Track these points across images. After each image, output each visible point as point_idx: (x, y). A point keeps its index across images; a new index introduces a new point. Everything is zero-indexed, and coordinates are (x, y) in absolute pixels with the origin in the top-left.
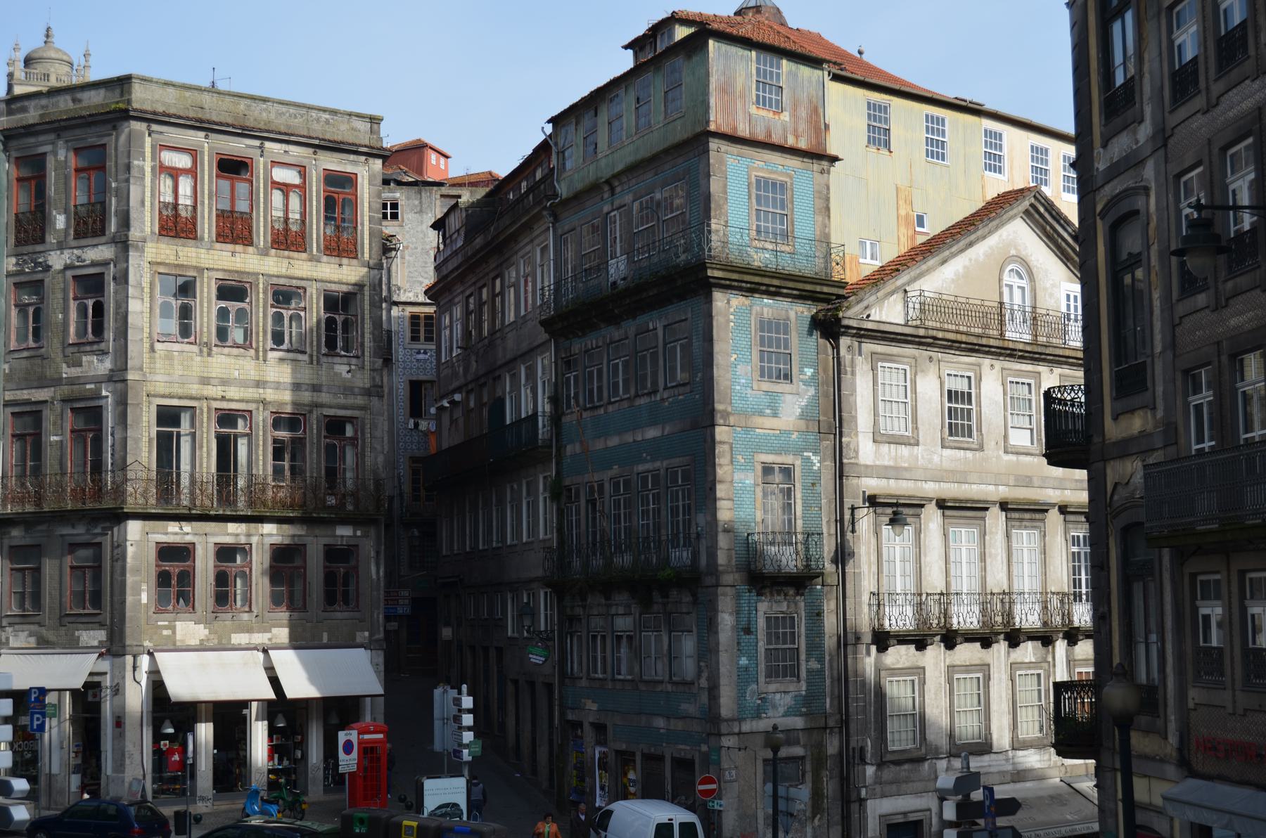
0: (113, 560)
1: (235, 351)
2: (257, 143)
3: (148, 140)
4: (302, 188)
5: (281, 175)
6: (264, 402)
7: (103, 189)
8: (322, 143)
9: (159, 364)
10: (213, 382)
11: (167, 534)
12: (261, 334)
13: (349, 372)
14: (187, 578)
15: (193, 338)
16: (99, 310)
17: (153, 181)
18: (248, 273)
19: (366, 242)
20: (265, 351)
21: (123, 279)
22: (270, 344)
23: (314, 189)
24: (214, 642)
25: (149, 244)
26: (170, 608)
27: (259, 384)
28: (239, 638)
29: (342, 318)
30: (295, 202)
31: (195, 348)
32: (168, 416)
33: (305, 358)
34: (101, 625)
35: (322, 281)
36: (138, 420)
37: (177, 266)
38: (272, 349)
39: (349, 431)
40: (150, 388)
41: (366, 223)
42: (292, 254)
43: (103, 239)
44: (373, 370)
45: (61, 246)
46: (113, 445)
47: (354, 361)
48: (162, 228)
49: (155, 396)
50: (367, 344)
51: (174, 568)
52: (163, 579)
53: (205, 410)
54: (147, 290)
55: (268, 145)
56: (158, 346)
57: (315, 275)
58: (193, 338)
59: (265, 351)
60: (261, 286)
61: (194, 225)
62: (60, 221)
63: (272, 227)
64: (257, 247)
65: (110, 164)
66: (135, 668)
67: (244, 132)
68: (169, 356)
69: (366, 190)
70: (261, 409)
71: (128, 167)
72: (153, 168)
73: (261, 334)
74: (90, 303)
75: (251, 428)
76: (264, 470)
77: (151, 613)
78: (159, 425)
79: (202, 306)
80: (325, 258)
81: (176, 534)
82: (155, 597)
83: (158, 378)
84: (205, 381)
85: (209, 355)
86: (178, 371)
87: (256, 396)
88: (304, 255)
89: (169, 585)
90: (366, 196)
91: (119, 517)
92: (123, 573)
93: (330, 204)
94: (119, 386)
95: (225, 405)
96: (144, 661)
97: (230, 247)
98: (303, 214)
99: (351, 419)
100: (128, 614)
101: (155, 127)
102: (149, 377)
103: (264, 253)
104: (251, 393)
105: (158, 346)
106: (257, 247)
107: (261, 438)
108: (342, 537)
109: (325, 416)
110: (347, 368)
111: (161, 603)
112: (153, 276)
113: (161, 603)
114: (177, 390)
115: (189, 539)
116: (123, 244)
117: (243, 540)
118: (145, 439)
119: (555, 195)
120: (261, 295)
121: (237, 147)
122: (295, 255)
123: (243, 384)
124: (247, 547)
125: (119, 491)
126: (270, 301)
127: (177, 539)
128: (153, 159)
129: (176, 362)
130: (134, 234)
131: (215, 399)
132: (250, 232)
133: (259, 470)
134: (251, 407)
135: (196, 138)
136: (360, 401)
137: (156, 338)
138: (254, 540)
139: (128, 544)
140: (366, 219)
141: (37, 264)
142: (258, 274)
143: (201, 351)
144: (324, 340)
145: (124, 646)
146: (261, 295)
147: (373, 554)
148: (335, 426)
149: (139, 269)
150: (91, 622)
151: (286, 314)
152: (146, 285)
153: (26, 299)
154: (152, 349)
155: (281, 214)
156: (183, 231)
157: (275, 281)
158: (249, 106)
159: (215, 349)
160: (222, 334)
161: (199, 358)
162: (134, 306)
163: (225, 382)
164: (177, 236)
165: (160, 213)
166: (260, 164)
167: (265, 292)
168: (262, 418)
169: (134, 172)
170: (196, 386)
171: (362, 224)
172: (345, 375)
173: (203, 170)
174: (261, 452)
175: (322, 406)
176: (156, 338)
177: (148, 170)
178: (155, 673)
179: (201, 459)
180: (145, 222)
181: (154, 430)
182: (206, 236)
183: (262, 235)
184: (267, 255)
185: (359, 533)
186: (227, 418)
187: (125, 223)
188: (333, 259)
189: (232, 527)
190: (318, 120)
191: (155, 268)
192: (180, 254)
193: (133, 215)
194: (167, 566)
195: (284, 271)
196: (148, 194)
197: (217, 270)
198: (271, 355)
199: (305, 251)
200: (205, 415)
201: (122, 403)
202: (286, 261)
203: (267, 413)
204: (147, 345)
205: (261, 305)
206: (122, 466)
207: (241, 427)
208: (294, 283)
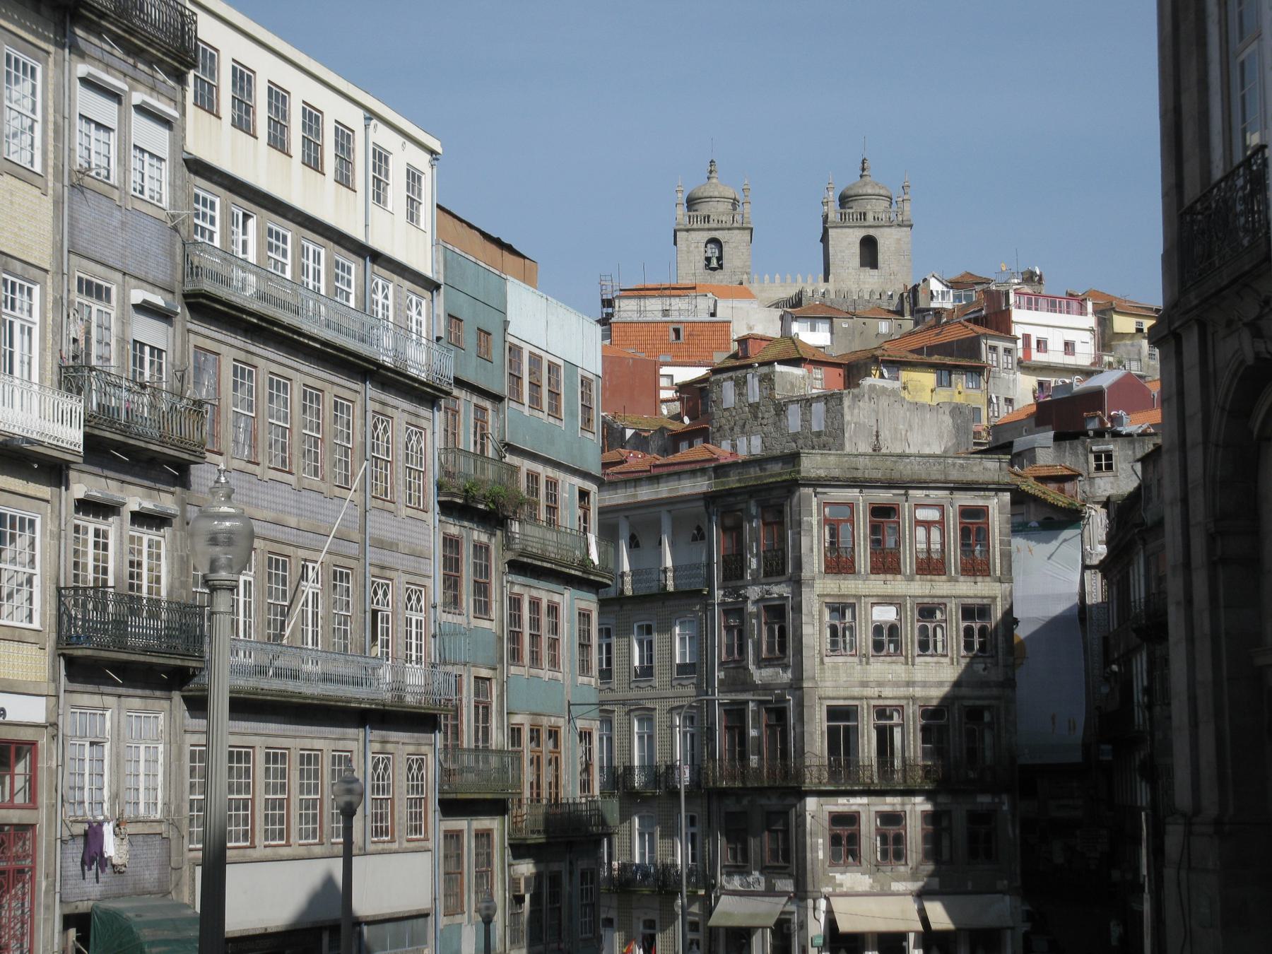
0: (797, 826)
1: (888, 659)
2: (903, 492)
3: (814, 500)
4: (941, 524)
5: (922, 514)
6: (913, 698)
7: (783, 539)
8: (956, 485)
9: (828, 674)
10: (871, 684)
11: (837, 805)
12: (909, 644)
13: (985, 669)
14: (854, 839)
15: (854, 651)
16: (783, 632)
17: (819, 532)
18: (898, 596)
19: (998, 561)
20: (913, 657)
21: (798, 609)
22: (917, 651)
23: (952, 522)
24: (877, 889)
25: (817, 581)
26: (842, 862)
27: (909, 684)
28: (897, 886)
29: (978, 625)
30: (935, 534)
31: (856, 659)
32: (835, 713)
33: (947, 660)
34: (790, 876)
35: (960, 597)
36: (812, 718)
37: (839, 596)
38: (919, 655)
39: (987, 717)
40: (822, 692)
41: (997, 546)
42: (933, 577)
43: (783, 578)
44: (1006, 666)
45: (755, 582)
46: (795, 737)
47: (989, 660)
48: (827, 567)
49: (825, 698)
50: (1000, 645)
51: (843, 831)
52: (835, 840)
53: (865, 707)
54: (817, 617)
55: (911, 492)
56: (826, 660)
57: (954, 592)
58: (854, 651)
59: (913, 657)
60: (908, 605)
61: (853, 562)
62: (754, 563)
63: (917, 557)
64: (904, 575)
65: (787, 520)
66: (815, 909)
67: (890, 485)
68: (835, 667)
69: (997, 519)
70: (911, 703)
71: (799, 524)
72: (819, 522)
73: (909, 644)
74: (776, 627)
75: (903, 720)
76: (915, 752)
77: (826, 866)
78: (829, 720)
79: (860, 625)
80: (962, 578)
81: (844, 805)
82: (829, 853)
83: (828, 684)
84: (864, 684)
85: (867, 663)
86: (843, 678)
87: (907, 694)
88: (944, 578)
89: (840, 844)
90: (997, 523)
91: (802, 795)
92: (804, 837)
93: (965, 532)
94: (798, 693)
95: (881, 702)
96: (822, 904)
97: (882, 576)
98: (943, 544)
99: (989, 707)
100: (809, 867)
101: (819, 490)
102: (820, 684)
103: (910, 579)
104: (902, 691)
105: (826, 660)
106: (904, 575)
107: (911, 727)
108: (982, 803)
109: (966, 707)
110: (983, 666)
111: (835, 859)
112: (821, 605)
113: (835, 859)
114: (842, 693)
115: (854, 808)
116: (797, 583)
117: (898, 808)
118: (818, 732)
119: (1143, 523)
120: (909, 613)
121: (884, 496)
122: (936, 578)
123: (896, 684)
124: (902, 814)
125: (799, 775)
126: (916, 616)
127: (845, 809)
128: (819, 514)
129: (841, 671)
130: (805, 574)
131: (872, 698)
132: (899, 563)
133: (910, 753)
134: (903, 702)
135: (855, 492)
136: (995, 692)
137: (824, 653)
138: (908, 808)
139: (807, 813)
140: (997, 542)
141: (739, 596)
142: (905, 596)
143: (861, 661)
144: (962, 644)
145: (806, 892)
146: (909, 613)
147: (1009, 817)
148: (974, 714)
149: (812, 603)
150: (782, 872)
151: (930, 626)
152: (816, 613)
153: (732, 622)
154: (822, 662)
155: (924, 546)
156: (844, 568)
157: (920, 600)
158: (896, 462)
159: (872, 660)
160: (878, 646)
161: (859, 667)
162: (807, 630)
163: (880, 684)
164: (839, 572)
165: (825, 555)
166: (906, 508)
167: (912, 610)
168: (912, 711)
169: (804, 526)
170: (857, 689)
171: (994, 547)
172: (981, 672)
173: (858, 518)
174: (911, 738)
175: (963, 698)
176: (824, 653)
177: (815, 523)
178: (830, 912)
179: (863, 746)
180: (814, 561)
181: (825, 724)
182: (863, 570)
183: (908, 564)
184: (912, 580)
185: (997, 800)
186: (882, 713)
187: (798, 566)
188: (969, 579)
189: (889, 799)
190: (954, 465)
191: (822, 599)
192: (842, 586)
193: (804, 559)
194: (838, 830)
195: (927, 592)
196: (815, 541)
197: (873, 596)
198: (918, 660)
199: (945, 574)
200: (865, 711)
201: (800, 705)
202: (929, 584)
203: (916, 707)
204: (817, 660)
205: (909, 621)
206: (801, 753)
207: (896, 719)
208: (936, 600)
